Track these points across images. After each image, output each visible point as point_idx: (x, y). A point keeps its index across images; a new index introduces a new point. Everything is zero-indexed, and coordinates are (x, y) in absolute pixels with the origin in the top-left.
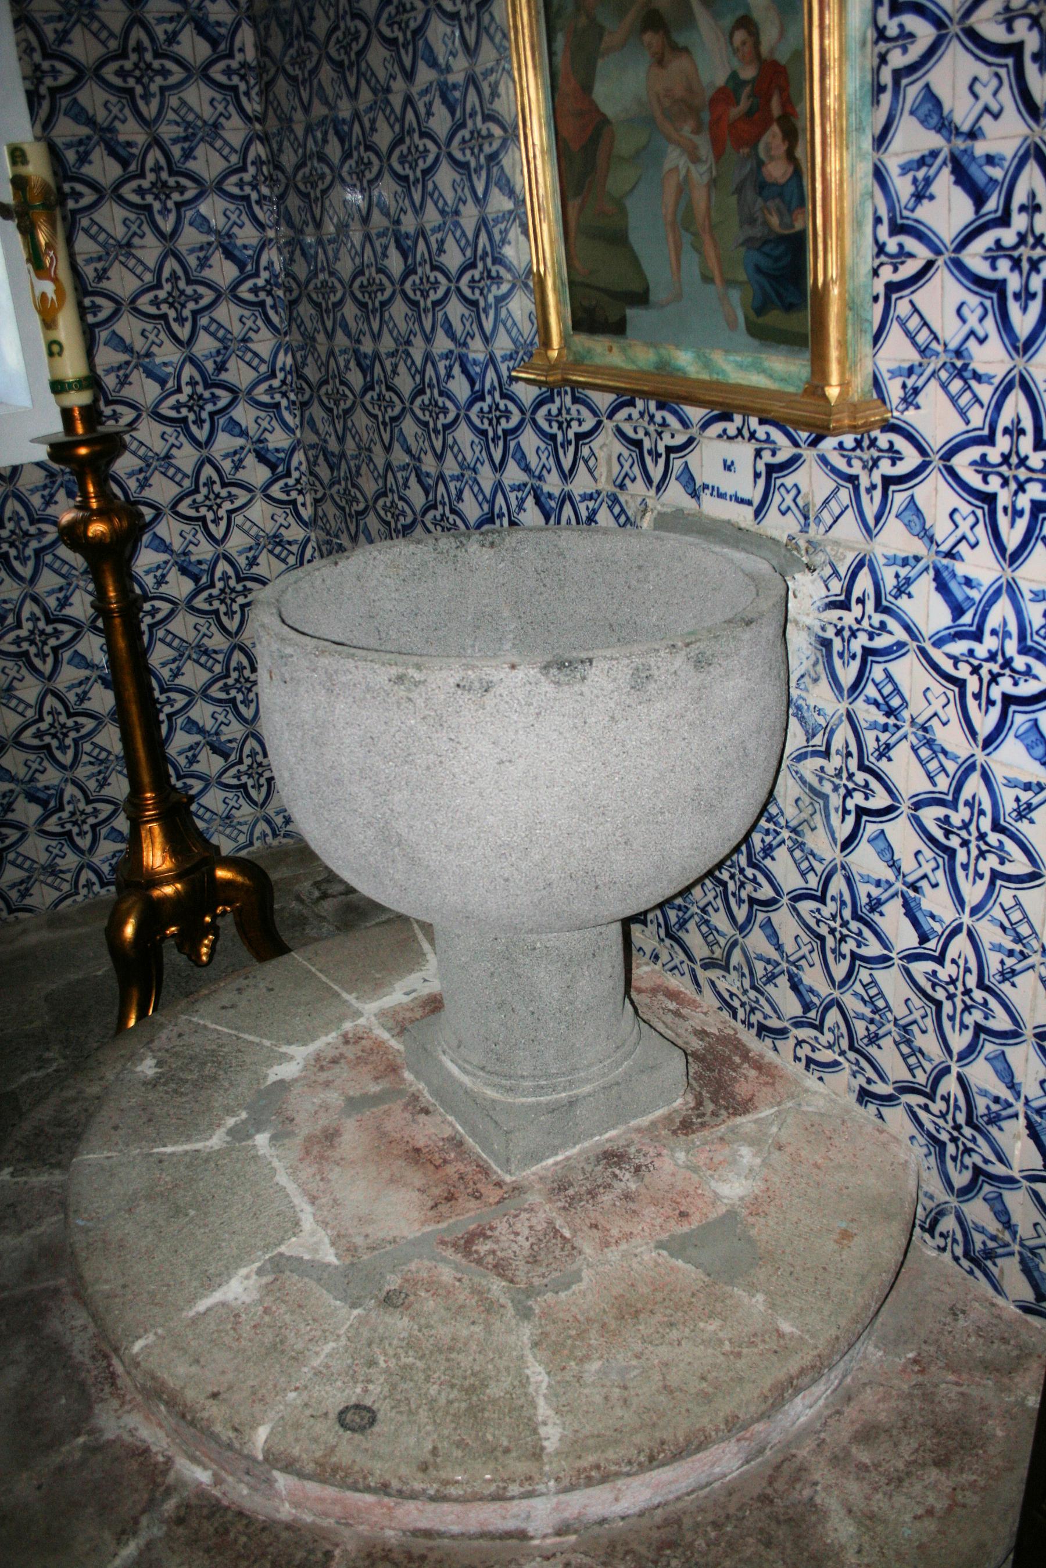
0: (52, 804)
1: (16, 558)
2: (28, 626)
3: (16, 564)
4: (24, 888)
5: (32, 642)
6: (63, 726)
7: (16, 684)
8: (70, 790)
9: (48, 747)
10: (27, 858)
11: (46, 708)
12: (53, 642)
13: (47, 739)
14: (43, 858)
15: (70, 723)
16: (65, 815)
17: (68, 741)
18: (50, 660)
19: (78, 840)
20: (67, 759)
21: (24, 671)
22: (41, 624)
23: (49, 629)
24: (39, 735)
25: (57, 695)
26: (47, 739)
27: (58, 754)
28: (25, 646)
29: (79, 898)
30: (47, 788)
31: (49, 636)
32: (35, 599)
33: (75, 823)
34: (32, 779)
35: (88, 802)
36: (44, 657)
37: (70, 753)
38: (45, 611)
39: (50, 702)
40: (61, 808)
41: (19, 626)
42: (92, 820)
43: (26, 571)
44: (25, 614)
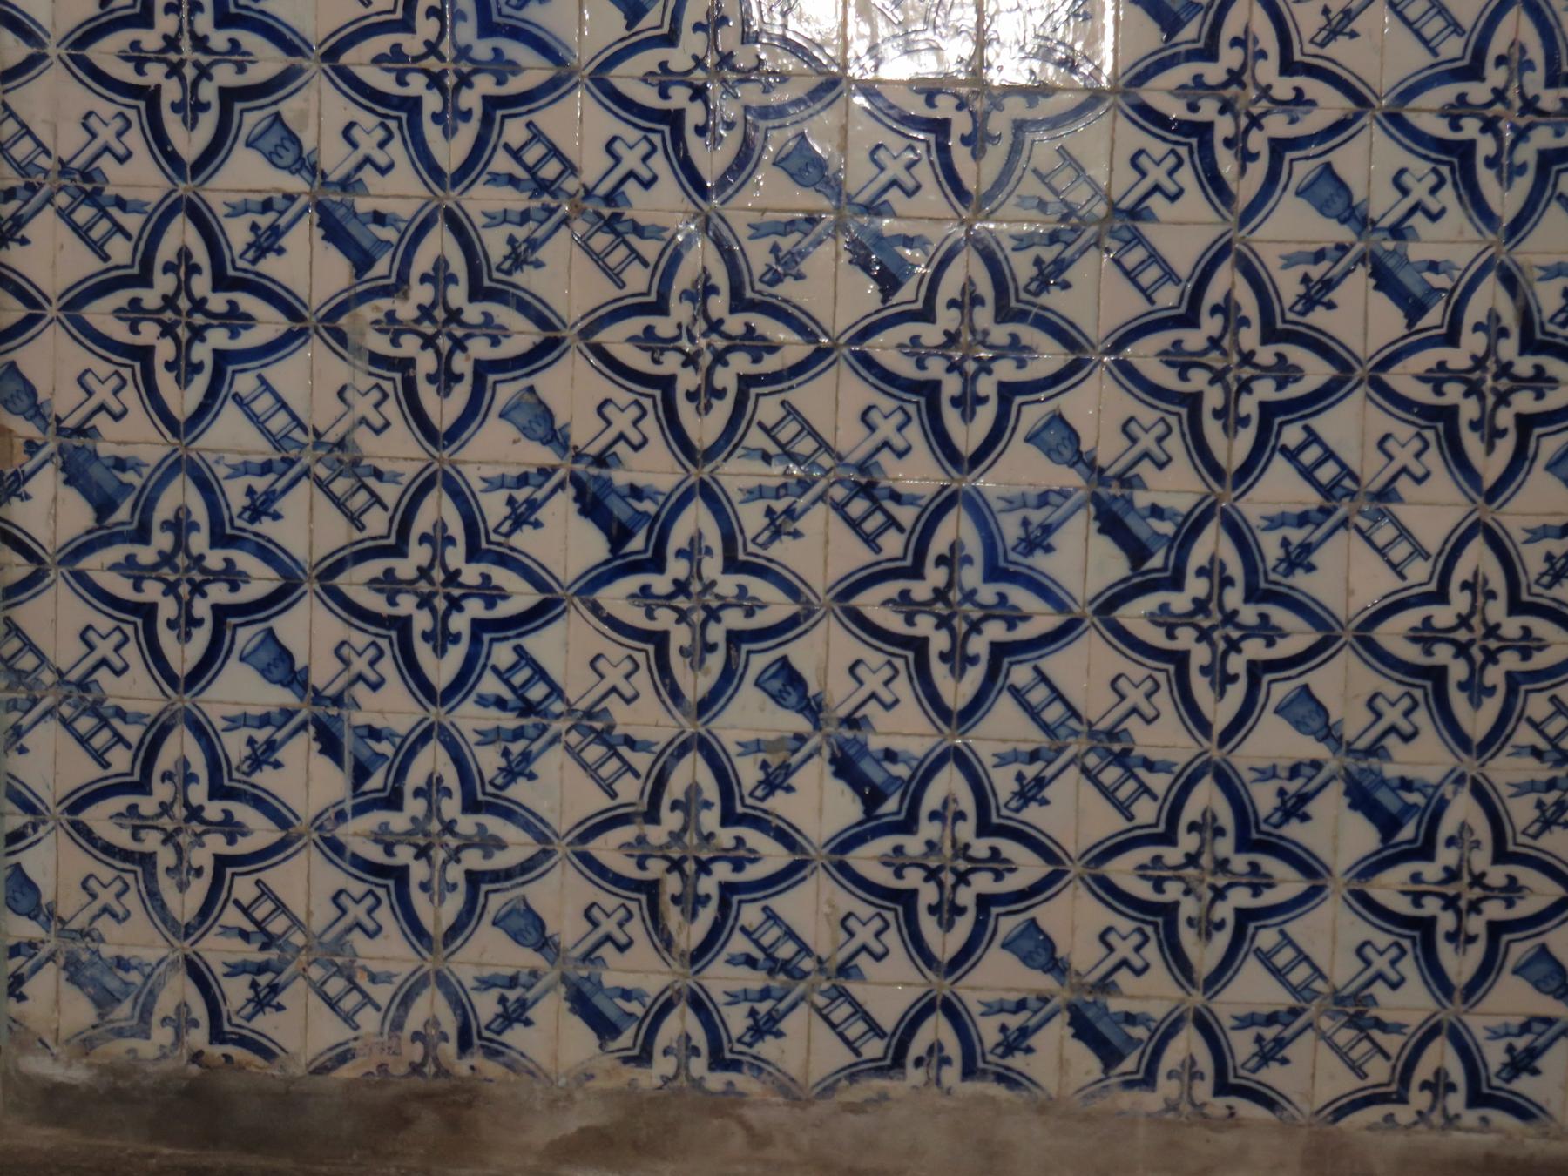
0: (1407, 832)
1: (1491, 162)
2: (1473, 342)
3: (1486, 178)
4: (1276, 1033)
5: (1473, 389)
6: (1492, 631)
7: (1404, 485)
8: (1463, 810)
9: (1438, 674)
10: (1303, 957)
12: (1524, 402)
13: (1443, 654)
14: (1344, 971)
15: (1512, 627)
16: (1431, 871)
17: (1494, 676)
18: (1506, 447)
19: (1446, 952)
20: (1477, 720)
22: (1508, 349)
23: (1524, 366)
24: (1425, 636)
25: (1496, 543)
26: (1443, 654)
27: (1459, 701)
28: (1453, 393)
29: (1404, 1114)
30: (1406, 784)
31: (1520, 383)
32: (1509, 280)
33: (1450, 903)
34: (1375, 750)
35: (1501, 855)
36: (1492, 435)
37: (1491, 707)
38: (1526, 318)
39: (1477, 557)
41: (1451, 338)
42: (1495, 910)
43: (1506, 200)
44: (1475, 311)
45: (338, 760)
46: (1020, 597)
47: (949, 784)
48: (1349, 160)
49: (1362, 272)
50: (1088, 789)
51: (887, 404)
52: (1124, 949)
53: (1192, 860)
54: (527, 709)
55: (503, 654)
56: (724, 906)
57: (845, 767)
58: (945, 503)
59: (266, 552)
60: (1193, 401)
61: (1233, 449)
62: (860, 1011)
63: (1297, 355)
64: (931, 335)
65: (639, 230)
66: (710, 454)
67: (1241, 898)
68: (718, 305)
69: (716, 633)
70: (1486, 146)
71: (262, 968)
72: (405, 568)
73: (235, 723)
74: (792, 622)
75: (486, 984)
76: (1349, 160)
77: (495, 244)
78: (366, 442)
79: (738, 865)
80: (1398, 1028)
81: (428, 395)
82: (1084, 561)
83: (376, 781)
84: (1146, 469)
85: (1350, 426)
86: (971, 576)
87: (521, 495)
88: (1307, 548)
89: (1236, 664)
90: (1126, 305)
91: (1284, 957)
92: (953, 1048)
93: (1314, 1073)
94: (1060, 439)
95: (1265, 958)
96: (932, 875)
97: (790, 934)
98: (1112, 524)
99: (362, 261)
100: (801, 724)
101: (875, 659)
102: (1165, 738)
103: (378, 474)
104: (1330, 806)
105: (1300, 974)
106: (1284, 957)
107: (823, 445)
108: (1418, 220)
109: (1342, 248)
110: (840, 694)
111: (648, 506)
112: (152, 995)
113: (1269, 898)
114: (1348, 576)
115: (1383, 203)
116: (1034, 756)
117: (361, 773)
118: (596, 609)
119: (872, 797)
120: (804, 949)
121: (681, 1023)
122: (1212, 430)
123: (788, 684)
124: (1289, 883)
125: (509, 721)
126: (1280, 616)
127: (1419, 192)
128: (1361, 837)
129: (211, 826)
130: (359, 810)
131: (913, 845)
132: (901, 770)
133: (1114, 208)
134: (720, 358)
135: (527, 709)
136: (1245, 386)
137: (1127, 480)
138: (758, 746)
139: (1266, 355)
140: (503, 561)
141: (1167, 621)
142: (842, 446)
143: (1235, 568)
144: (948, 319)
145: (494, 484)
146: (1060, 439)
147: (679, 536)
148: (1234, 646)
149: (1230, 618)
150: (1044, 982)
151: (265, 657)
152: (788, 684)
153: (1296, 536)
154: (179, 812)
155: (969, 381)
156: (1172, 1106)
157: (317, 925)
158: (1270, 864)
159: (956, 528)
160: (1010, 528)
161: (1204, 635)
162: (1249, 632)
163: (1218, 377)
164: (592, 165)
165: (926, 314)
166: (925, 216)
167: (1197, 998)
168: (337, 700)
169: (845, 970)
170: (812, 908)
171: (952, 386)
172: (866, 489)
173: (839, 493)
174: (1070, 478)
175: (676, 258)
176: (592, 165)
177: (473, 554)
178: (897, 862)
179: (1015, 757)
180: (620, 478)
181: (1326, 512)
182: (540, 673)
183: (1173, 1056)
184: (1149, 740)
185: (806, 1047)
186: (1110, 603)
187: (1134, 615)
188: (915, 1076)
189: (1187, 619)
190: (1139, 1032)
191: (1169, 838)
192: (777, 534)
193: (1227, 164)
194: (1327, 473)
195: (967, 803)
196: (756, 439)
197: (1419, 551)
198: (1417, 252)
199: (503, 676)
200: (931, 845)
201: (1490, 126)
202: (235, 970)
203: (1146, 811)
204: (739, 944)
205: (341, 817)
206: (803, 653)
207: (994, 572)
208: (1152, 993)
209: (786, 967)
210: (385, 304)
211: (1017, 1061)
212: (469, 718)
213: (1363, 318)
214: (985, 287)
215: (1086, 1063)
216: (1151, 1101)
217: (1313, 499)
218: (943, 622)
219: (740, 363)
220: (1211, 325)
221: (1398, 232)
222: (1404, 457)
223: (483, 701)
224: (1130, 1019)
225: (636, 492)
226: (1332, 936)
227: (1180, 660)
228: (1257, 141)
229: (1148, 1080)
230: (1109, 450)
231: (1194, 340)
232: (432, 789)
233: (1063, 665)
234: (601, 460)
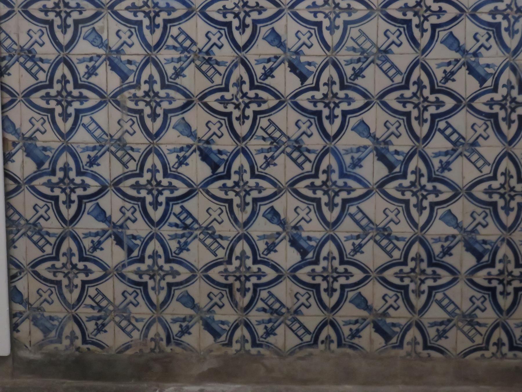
0: (486, 258)
1: (506, 30)
2: (502, 91)
3: (505, 35)
4: (443, 328)
5: (503, 107)
7: (481, 141)
8: (504, 250)
9: (494, 205)
10: (451, 302)
11: (502, 169)
13: (496, 197)
14: (466, 307)
16: (494, 271)
19: (500, 299)
21: (490, 131)
24: (489, 191)
26: (496, 197)
27: (502, 213)
28: (496, 108)
29: (488, 354)
30: (485, 242)
33: (501, 282)
34: (474, 231)
40: (492, 265)
41: (495, 90)
44: (503, 80)
45: (122, 246)
46: (351, 183)
47: (329, 247)
48: (458, 31)
49: (464, 69)
50: (377, 249)
51: (304, 119)
52: (391, 301)
53: (413, 270)
54: (186, 227)
55: (177, 209)
56: (255, 291)
57: (294, 243)
58: (325, 152)
59: (95, 177)
60: (408, 115)
61: (422, 130)
62: (302, 326)
63: (442, 97)
64: (318, 95)
65: (218, 63)
66: (245, 138)
67: (430, 282)
68: (246, 88)
69: (249, 199)
70: (505, 24)
71: (99, 318)
72: (143, 181)
73: (87, 235)
74: (275, 194)
75: (175, 321)
76: (458, 31)
77: (169, 70)
78: (128, 138)
79: (259, 278)
80: (484, 325)
81: (148, 122)
82: (373, 170)
83: (135, 253)
84: (393, 138)
85: (461, 121)
86: (335, 177)
87: (181, 154)
88: (448, 163)
89: (426, 203)
90: (384, 83)
91: (445, 302)
92: (334, 336)
93: (457, 341)
94: (363, 129)
95: (439, 303)
96: (325, 278)
97: (278, 300)
98: (382, 157)
99: (124, 77)
100: (279, 229)
101: (303, 206)
102: (403, 229)
103: (132, 149)
104: (459, 250)
105: (451, 308)
106: (445, 302)
107: (283, 134)
108: (482, 50)
109: (457, 61)
110: (292, 218)
111: (224, 157)
112: (62, 329)
113: (440, 282)
114: (462, 172)
115: (470, 45)
116: (358, 237)
117: (130, 251)
118: (208, 192)
119: (304, 253)
120: (282, 305)
121: (241, 332)
122: (415, 124)
123: (273, 215)
124: (446, 277)
125: (180, 232)
126: (440, 186)
127: (482, 40)
128: (470, 261)
129: (80, 271)
130: (130, 263)
131: (318, 269)
132: (313, 243)
133: (379, 50)
134: (247, 106)
135: (186, 227)
136: (425, 109)
137: (387, 142)
138: (264, 237)
139: (432, 98)
140: (176, 177)
141: (401, 189)
142: (290, 134)
143: (424, 171)
144: (324, 89)
145: (171, 151)
146: (363, 129)
147: (235, 167)
148: (425, 197)
149: (423, 188)
150: (364, 313)
151: (96, 213)
152: (273, 215)
153: (445, 159)
154: (69, 266)
155: (332, 110)
156: (409, 354)
157: (117, 303)
158: (439, 271)
159: (329, 160)
160: (347, 160)
161: (414, 194)
162: (430, 192)
163: (416, 106)
164: (201, 41)
165: (316, 88)
166: (315, 54)
167: (416, 317)
168: (121, 226)
169: (296, 312)
170: (284, 291)
171: (326, 112)
172: (298, 149)
173: (289, 150)
174: (367, 142)
175: (231, 73)
176: (201, 41)
177: (166, 175)
178: (313, 274)
179: (352, 237)
180: (214, 148)
181: (454, 151)
182: (190, 215)
183: (408, 337)
184: (395, 230)
185: (284, 338)
186: (382, 185)
187: (391, 188)
188: (321, 347)
189: (408, 188)
190: (397, 329)
191: (405, 263)
192: (268, 165)
193: (417, 33)
194: (454, 137)
195: (336, 254)
196: (260, 132)
197: (486, 163)
198: (482, 61)
199: (177, 216)
200: (324, 268)
201: (506, 17)
202: (90, 319)
203: (396, 254)
204: (260, 304)
205: (124, 266)
206: (279, 205)
207: (342, 175)
208: (401, 315)
209: (276, 311)
210: (133, 91)
211: (356, 341)
212: (166, 231)
213: (465, 84)
214: (336, 78)
215: (379, 340)
216: (402, 352)
217: (449, 146)
218: (326, 193)
219: (254, 107)
220: (413, 88)
221: (476, 54)
222: (480, 131)
223: (171, 225)
224: (394, 325)
225: (220, 152)
226: (461, 294)
227: (407, 202)
228: (427, 25)
229: (400, 345)
230: (380, 133)
231: (408, 94)
232: (154, 256)
233: (367, 206)
234: (208, 142)
